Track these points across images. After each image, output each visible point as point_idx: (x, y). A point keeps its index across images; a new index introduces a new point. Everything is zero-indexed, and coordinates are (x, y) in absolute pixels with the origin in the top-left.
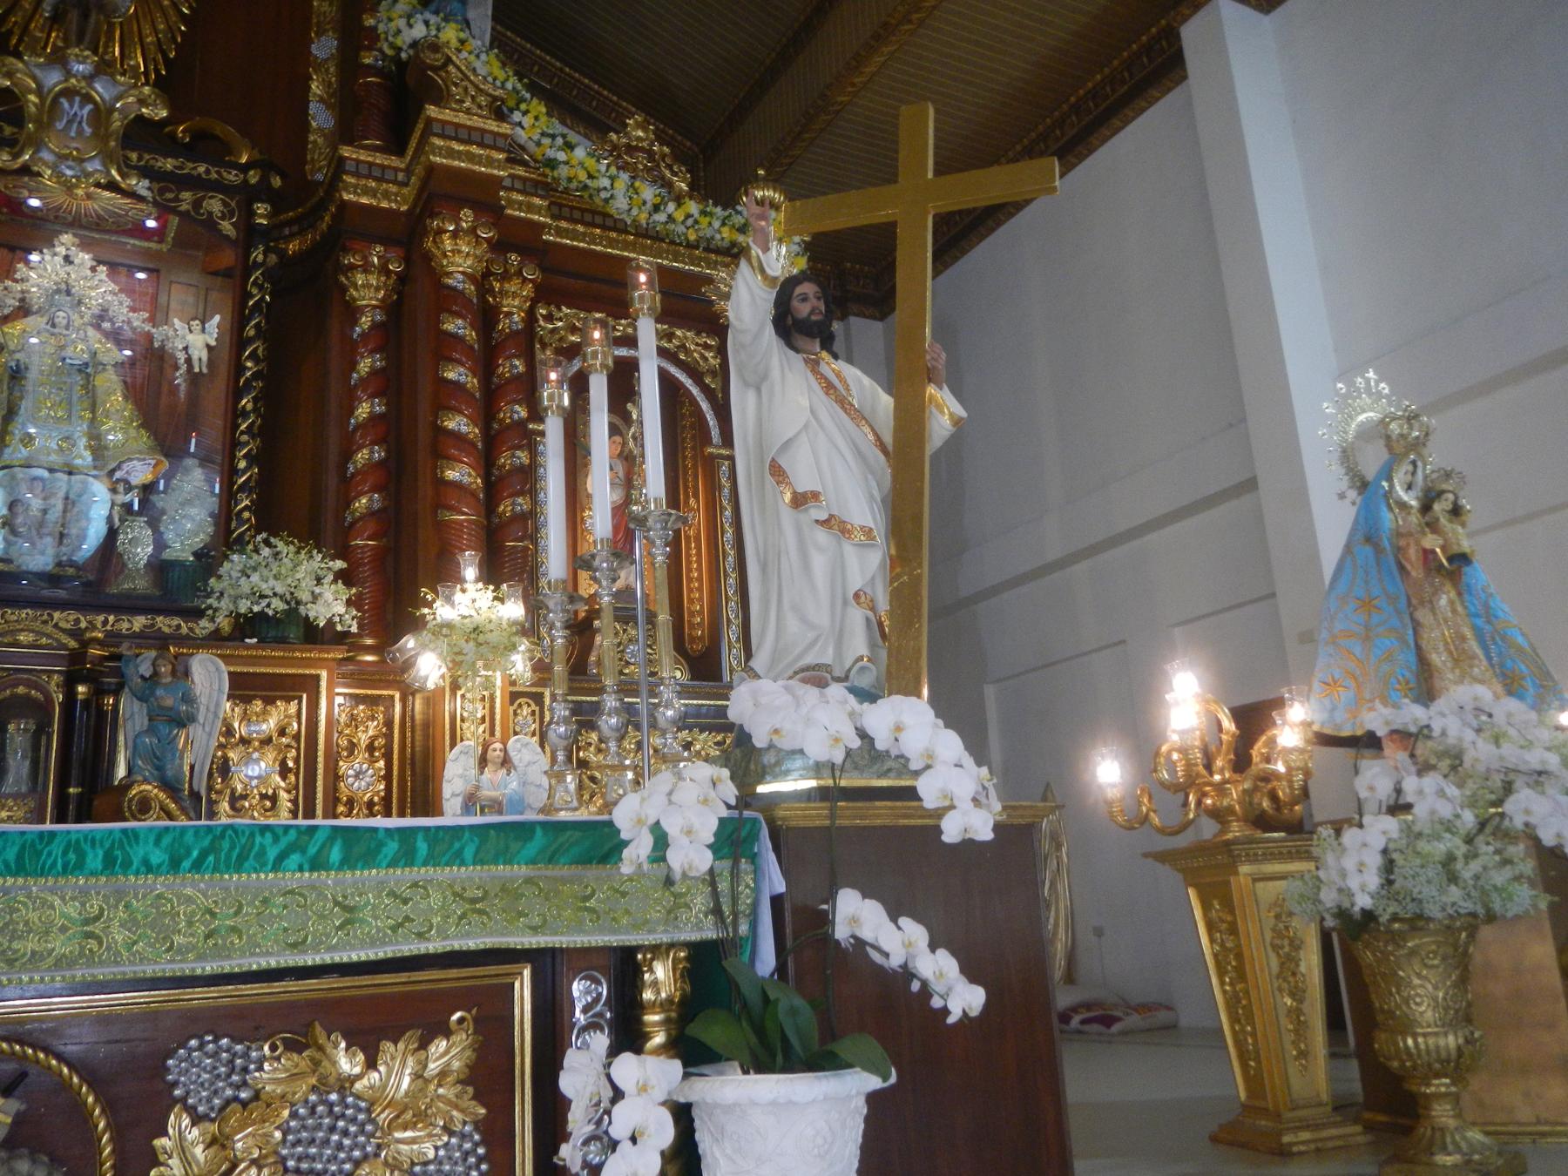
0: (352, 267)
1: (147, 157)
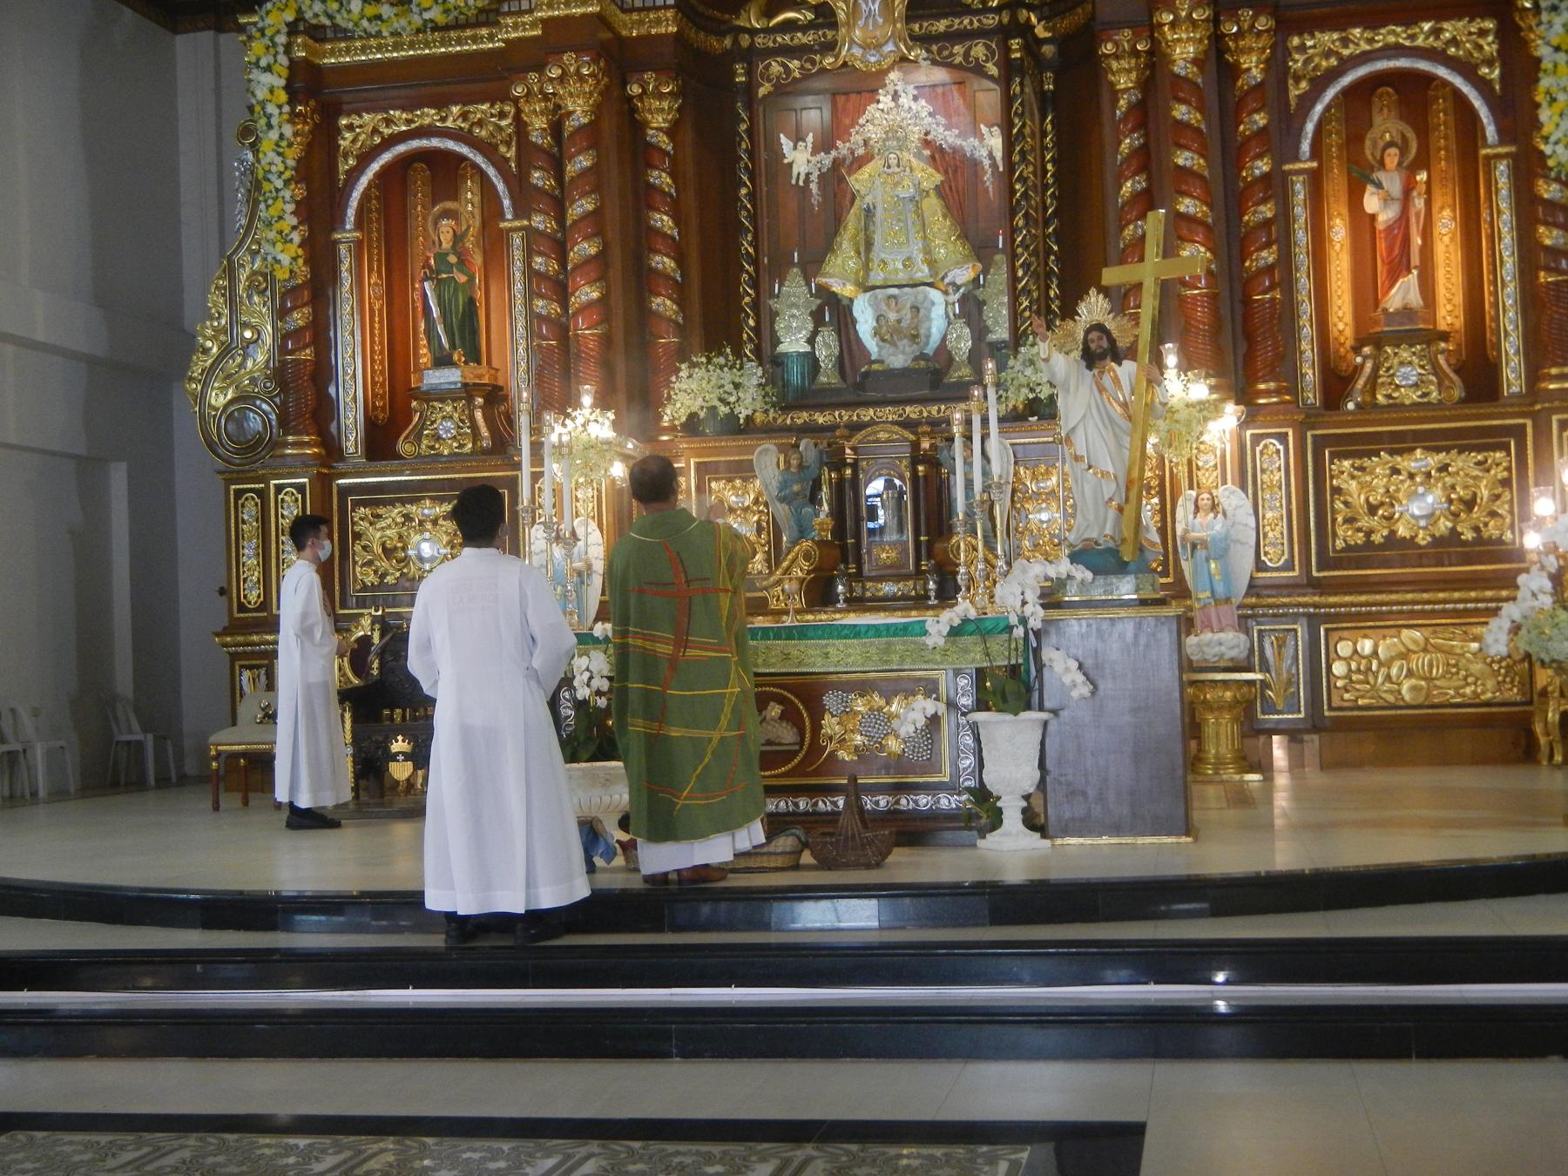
0: (1107, 56)
1: (925, 24)
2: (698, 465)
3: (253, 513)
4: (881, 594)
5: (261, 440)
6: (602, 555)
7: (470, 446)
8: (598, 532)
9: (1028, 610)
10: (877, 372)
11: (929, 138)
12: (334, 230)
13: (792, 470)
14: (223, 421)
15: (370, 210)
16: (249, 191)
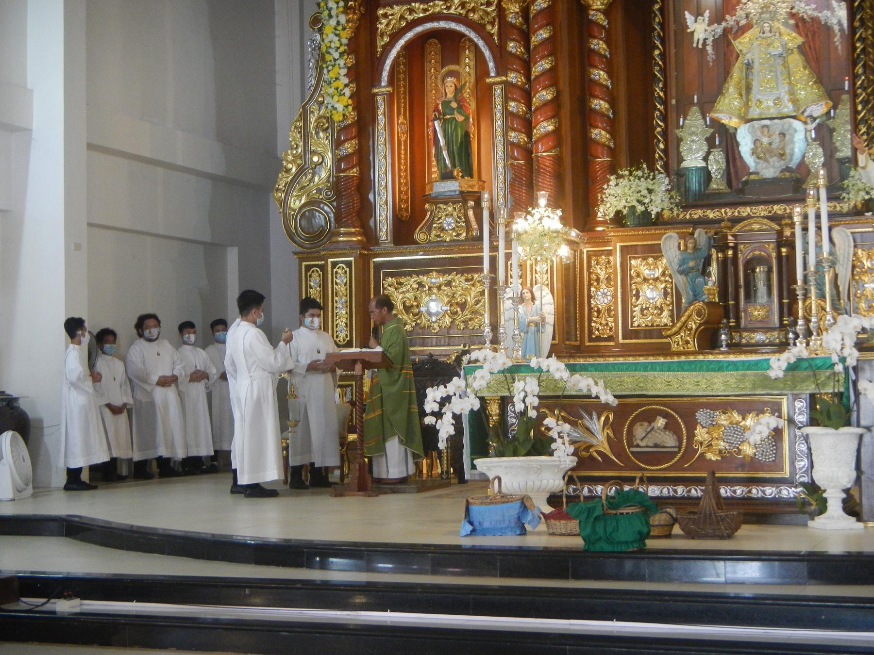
2: (622, 248)
3: (317, 281)
4: (753, 341)
5: (323, 231)
6: (553, 312)
7: (464, 234)
8: (550, 296)
9: (846, 352)
10: (754, 181)
11: (794, 11)
12: (373, 86)
13: (689, 251)
14: (298, 218)
15: (399, 73)
16: (318, 61)
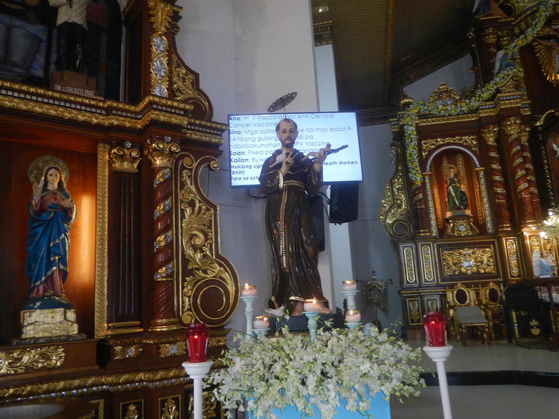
16: (395, 162)
